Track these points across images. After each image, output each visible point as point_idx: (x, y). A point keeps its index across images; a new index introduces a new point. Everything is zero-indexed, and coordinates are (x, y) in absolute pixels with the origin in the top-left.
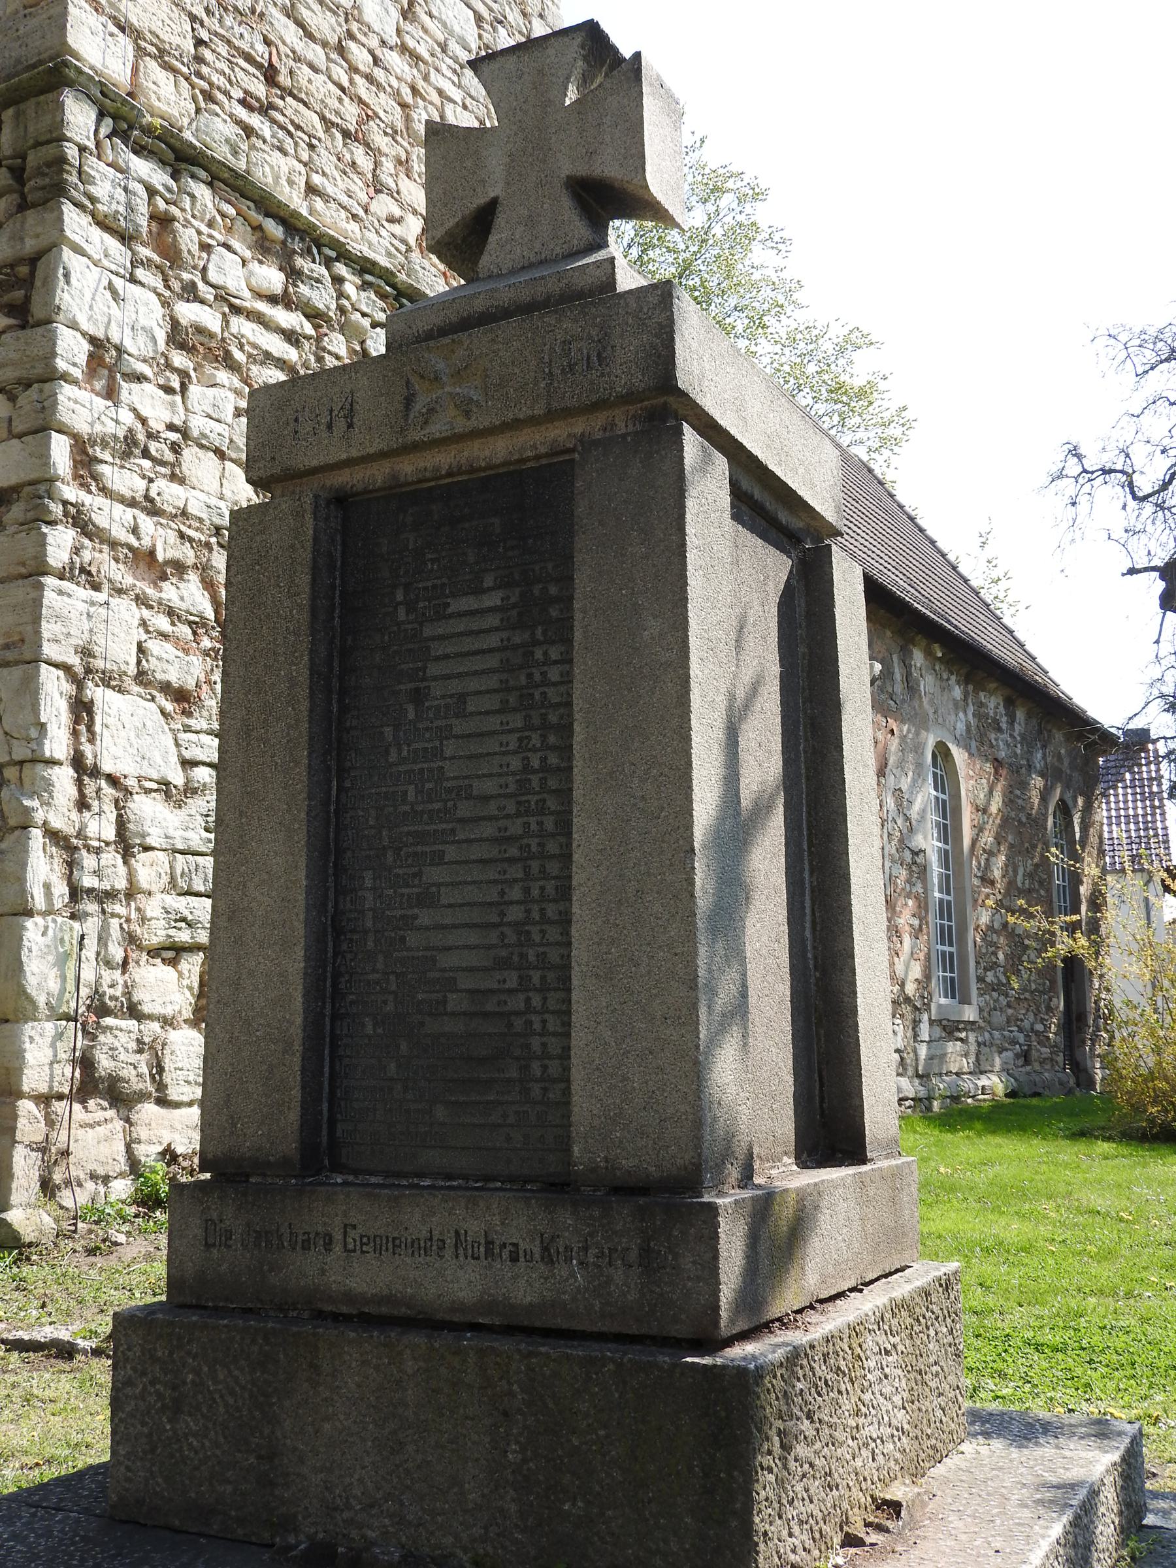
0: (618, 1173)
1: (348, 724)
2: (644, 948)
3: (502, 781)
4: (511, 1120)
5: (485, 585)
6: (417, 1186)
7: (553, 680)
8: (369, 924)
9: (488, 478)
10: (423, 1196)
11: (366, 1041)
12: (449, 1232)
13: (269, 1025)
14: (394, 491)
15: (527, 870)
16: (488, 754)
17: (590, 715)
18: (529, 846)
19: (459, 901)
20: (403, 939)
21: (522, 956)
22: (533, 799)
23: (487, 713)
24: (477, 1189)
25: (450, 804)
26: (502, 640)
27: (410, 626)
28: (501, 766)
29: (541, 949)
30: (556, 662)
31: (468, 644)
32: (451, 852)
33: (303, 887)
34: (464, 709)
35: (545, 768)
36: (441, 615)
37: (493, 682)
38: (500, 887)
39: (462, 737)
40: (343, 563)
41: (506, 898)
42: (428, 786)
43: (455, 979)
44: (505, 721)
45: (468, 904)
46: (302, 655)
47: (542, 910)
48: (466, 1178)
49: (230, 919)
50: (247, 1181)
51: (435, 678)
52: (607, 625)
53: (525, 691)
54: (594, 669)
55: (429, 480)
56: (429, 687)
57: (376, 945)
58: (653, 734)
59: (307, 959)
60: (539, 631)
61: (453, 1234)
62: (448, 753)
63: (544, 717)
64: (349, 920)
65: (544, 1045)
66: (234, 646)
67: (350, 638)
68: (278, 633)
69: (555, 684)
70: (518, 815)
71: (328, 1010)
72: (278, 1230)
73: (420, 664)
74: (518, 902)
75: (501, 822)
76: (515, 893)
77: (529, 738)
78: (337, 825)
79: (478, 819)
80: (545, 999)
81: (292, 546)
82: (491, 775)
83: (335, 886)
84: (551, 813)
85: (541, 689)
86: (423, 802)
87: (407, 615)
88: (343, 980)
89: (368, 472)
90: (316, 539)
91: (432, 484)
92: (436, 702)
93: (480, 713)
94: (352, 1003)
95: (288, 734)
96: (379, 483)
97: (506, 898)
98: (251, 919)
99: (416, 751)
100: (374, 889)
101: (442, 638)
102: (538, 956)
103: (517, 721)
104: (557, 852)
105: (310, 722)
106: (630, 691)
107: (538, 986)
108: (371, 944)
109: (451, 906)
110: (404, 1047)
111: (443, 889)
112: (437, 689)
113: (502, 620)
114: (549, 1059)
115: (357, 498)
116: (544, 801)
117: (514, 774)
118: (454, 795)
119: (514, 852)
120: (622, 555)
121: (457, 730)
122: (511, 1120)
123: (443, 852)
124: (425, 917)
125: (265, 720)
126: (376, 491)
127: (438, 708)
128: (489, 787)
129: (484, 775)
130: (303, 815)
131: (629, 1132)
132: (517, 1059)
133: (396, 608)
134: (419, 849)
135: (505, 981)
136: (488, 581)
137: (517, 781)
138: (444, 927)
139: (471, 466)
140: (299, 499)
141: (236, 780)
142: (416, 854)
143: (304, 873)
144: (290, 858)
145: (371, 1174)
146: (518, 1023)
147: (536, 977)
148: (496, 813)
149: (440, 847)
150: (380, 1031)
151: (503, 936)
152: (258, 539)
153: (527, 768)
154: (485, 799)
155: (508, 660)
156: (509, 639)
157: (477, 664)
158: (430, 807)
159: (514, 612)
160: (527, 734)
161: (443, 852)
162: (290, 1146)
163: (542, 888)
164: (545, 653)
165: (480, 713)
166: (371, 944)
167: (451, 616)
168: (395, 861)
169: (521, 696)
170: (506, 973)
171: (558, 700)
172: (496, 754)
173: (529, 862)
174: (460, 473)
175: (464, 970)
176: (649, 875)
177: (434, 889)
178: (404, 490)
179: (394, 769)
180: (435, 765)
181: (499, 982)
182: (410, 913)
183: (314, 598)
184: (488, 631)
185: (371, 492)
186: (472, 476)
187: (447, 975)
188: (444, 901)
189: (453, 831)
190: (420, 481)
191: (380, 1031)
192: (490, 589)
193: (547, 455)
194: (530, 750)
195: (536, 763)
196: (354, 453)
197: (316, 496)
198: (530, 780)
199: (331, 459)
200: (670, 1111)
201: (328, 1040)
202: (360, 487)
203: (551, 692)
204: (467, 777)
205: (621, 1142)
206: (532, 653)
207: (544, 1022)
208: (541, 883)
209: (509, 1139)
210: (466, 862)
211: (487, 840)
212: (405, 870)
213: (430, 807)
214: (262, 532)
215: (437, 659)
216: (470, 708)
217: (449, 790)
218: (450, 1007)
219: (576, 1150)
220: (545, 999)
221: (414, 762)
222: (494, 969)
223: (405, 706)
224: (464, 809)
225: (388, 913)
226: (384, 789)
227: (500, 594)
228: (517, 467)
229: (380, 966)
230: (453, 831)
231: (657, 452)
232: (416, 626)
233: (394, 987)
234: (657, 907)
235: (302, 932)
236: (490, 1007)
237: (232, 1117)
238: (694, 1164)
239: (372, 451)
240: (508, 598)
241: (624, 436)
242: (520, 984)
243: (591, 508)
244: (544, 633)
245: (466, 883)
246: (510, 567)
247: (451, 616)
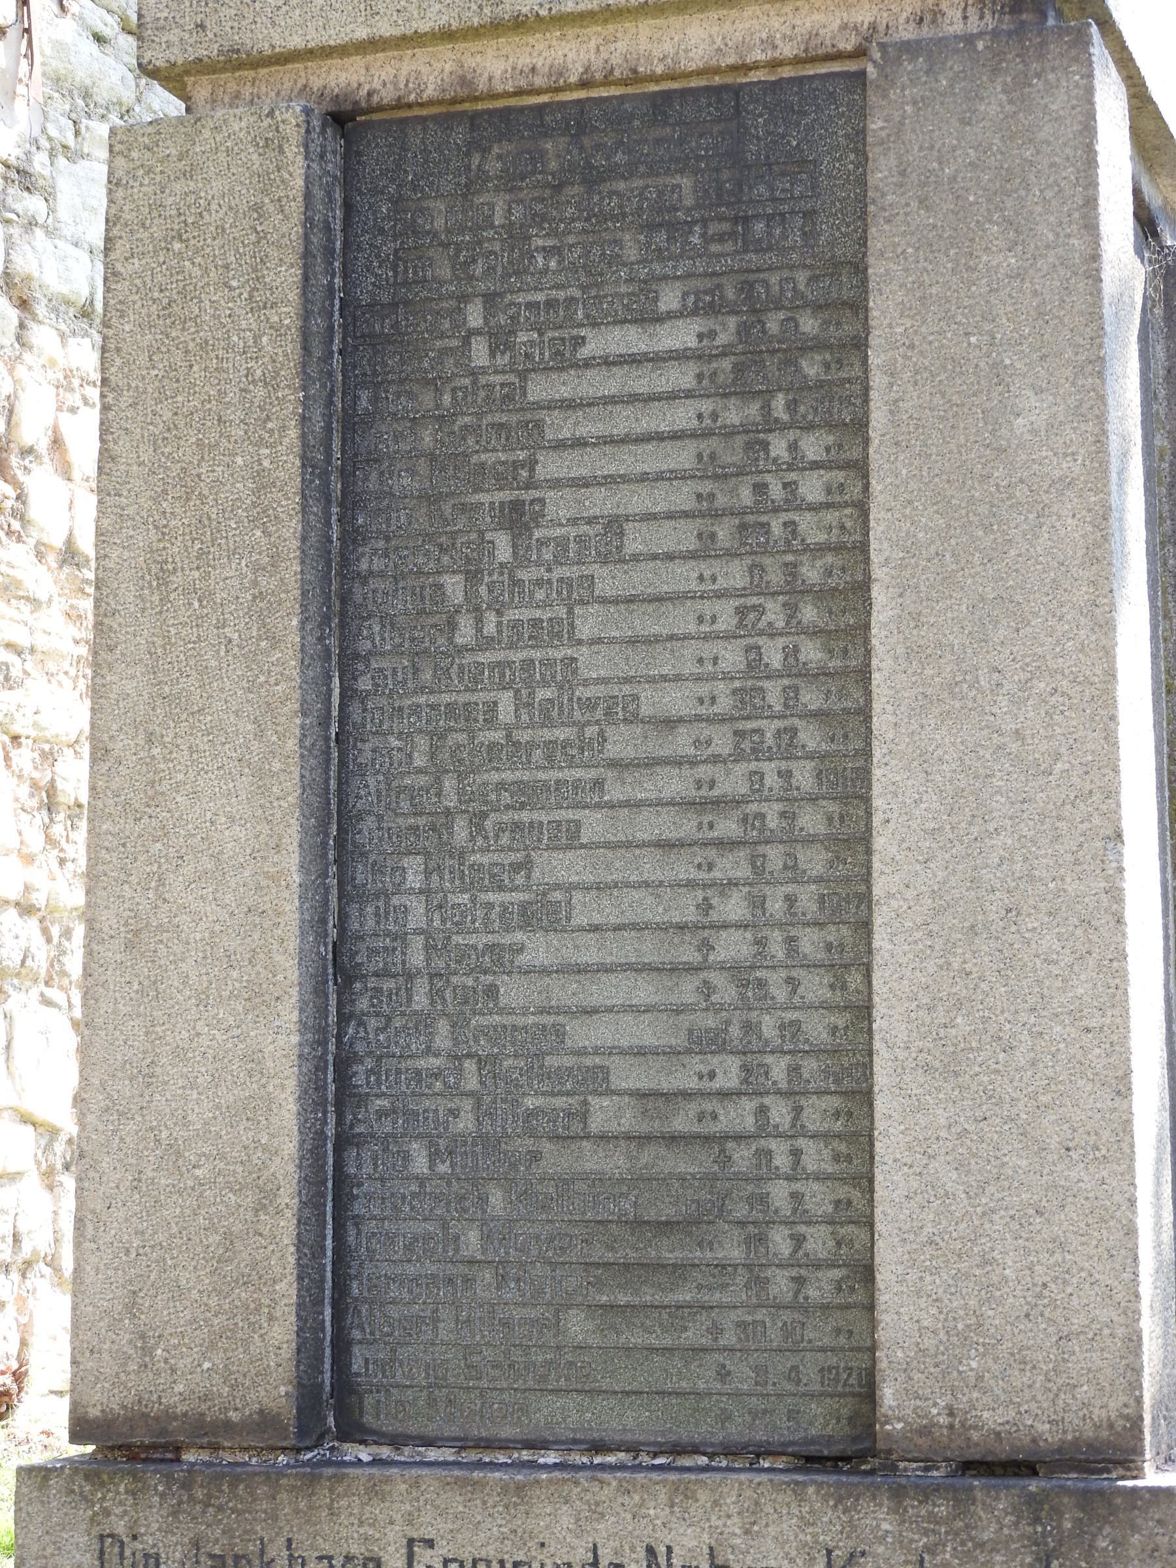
0: (975, 1436)
1: (364, 566)
2: (1023, 1017)
3: (704, 689)
4: (729, 1338)
5: (663, 307)
6: (532, 1465)
7: (810, 498)
8: (417, 958)
9: (667, 95)
10: (577, 1483)
11: (414, 1188)
12: (633, 1549)
13: (222, 1157)
14: (459, 108)
15: (758, 865)
16: (672, 637)
17: (906, 574)
18: (762, 816)
19: (613, 920)
20: (492, 992)
21: (749, 1027)
22: (770, 727)
23: (670, 557)
24: (660, 1468)
25: (591, 731)
26: (700, 416)
27: (498, 379)
28: (700, 661)
29: (790, 1016)
30: (815, 465)
31: (624, 421)
32: (594, 825)
33: (295, 887)
34: (619, 548)
35: (795, 670)
36: (565, 360)
37: (682, 497)
38: (700, 894)
39: (616, 601)
40: (346, 245)
41: (714, 916)
42: (542, 694)
43: (605, 1071)
44: (707, 574)
45: (634, 927)
46: (284, 428)
47: (791, 940)
48: (633, 1448)
49: (129, 946)
50: (178, 1460)
51: (555, 484)
52: (938, 400)
53: (750, 518)
54: (913, 485)
55: (539, 92)
56: (542, 501)
57: (433, 1003)
58: (1036, 615)
59: (303, 1027)
60: (779, 403)
61: (642, 1553)
62: (585, 630)
63: (791, 570)
64: (373, 952)
65: (796, 1196)
66: (127, 398)
67: (364, 396)
68: (228, 381)
69: (813, 508)
70: (738, 756)
71: (330, 1130)
72: (262, 1552)
73: (522, 455)
74: (742, 926)
75: (702, 768)
76: (734, 907)
77: (760, 610)
78: (342, 763)
79: (652, 763)
80: (798, 1110)
81: (257, 208)
82: (678, 678)
83: (341, 884)
84: (810, 757)
85: (784, 517)
86: (531, 726)
87: (492, 354)
88: (359, 1068)
89: (406, 68)
90: (308, 195)
91: (544, 99)
92: (558, 532)
93: (655, 557)
94: (381, 1114)
95: (255, 583)
96: (430, 92)
97: (714, 916)
98: (178, 949)
99: (515, 625)
100: (426, 892)
101: (568, 405)
102: (782, 1027)
103: (735, 575)
104: (822, 829)
105: (302, 562)
106: (988, 529)
107: (783, 1085)
108: (420, 1000)
109: (595, 928)
110: (496, 1199)
111: (577, 896)
112: (559, 506)
113: (700, 377)
114: (809, 1223)
115: (375, 117)
116: (794, 731)
117: (727, 677)
118: (599, 714)
119: (728, 827)
120: (969, 268)
121: (604, 587)
122: (729, 1338)
123: (578, 824)
124: (539, 949)
125: (201, 554)
126: (421, 105)
127: (562, 543)
128: (676, 700)
129: (665, 678)
130: (292, 745)
131: (996, 1360)
132: (742, 1224)
133: (466, 341)
134: (525, 816)
135: (712, 1075)
136: (669, 299)
137: (735, 692)
138: (581, 970)
139: (635, 71)
140: (271, 114)
141: (139, 669)
142: (517, 826)
143: (295, 859)
144: (265, 829)
145: (429, 1443)
146: (742, 1157)
147: (779, 1068)
148: (692, 751)
149: (571, 815)
150: (443, 1168)
151: (708, 989)
152: (178, 187)
153: (755, 665)
154: (669, 723)
155: (713, 456)
156: (714, 416)
157: (649, 459)
158: (547, 734)
159: (726, 364)
160: (754, 600)
161: (578, 824)
162: (276, 1391)
163: (790, 900)
164: (793, 447)
165: (655, 557)
166: (420, 1000)
167: (587, 364)
168: (472, 839)
169: (743, 527)
170: (715, 1060)
171: (822, 537)
172: (686, 637)
173: (761, 849)
174: (607, 82)
175: (623, 1052)
176: (1031, 878)
177: (557, 895)
178: (480, 106)
179: (468, 659)
180: (559, 655)
181: (701, 1077)
182: (507, 940)
183: (306, 315)
184: (672, 396)
185: (409, 106)
186: (630, 90)
187: (588, 1061)
188: (580, 920)
189: (598, 784)
190: (519, 93)
191: (443, 1168)
192: (670, 316)
193: (797, 61)
194: (761, 633)
195: (774, 658)
196: (385, 29)
197: (307, 112)
198: (761, 689)
199: (333, 37)
200: (1078, 1321)
201: (330, 1184)
202: (387, 96)
203: (805, 522)
204: (627, 680)
205: (979, 1378)
206: (765, 445)
207: (796, 1153)
208: (789, 889)
209: (723, 1374)
210: (628, 845)
211: (671, 803)
212: (496, 857)
213: (547, 734)
214: (187, 175)
215: (560, 445)
216: (633, 546)
217: (590, 705)
218: (594, 1127)
219: (888, 1395)
220: (798, 1110)
221: (511, 646)
222: (689, 1051)
223: (488, 536)
224: (622, 742)
225: (458, 939)
226: (446, 698)
227: (696, 325)
228: (729, 80)
229: (442, 1039)
230: (598, 784)
231: (1038, 75)
232: (512, 378)
233: (472, 1084)
234: (1049, 942)
235: (294, 975)
236: (681, 1123)
237: (143, 1336)
238: (1127, 1418)
239: (424, 27)
240: (712, 334)
241: (970, 39)
242: (746, 1081)
243: (903, 173)
244: (792, 406)
245: (628, 885)
246: (714, 274)
247: (587, 364)
